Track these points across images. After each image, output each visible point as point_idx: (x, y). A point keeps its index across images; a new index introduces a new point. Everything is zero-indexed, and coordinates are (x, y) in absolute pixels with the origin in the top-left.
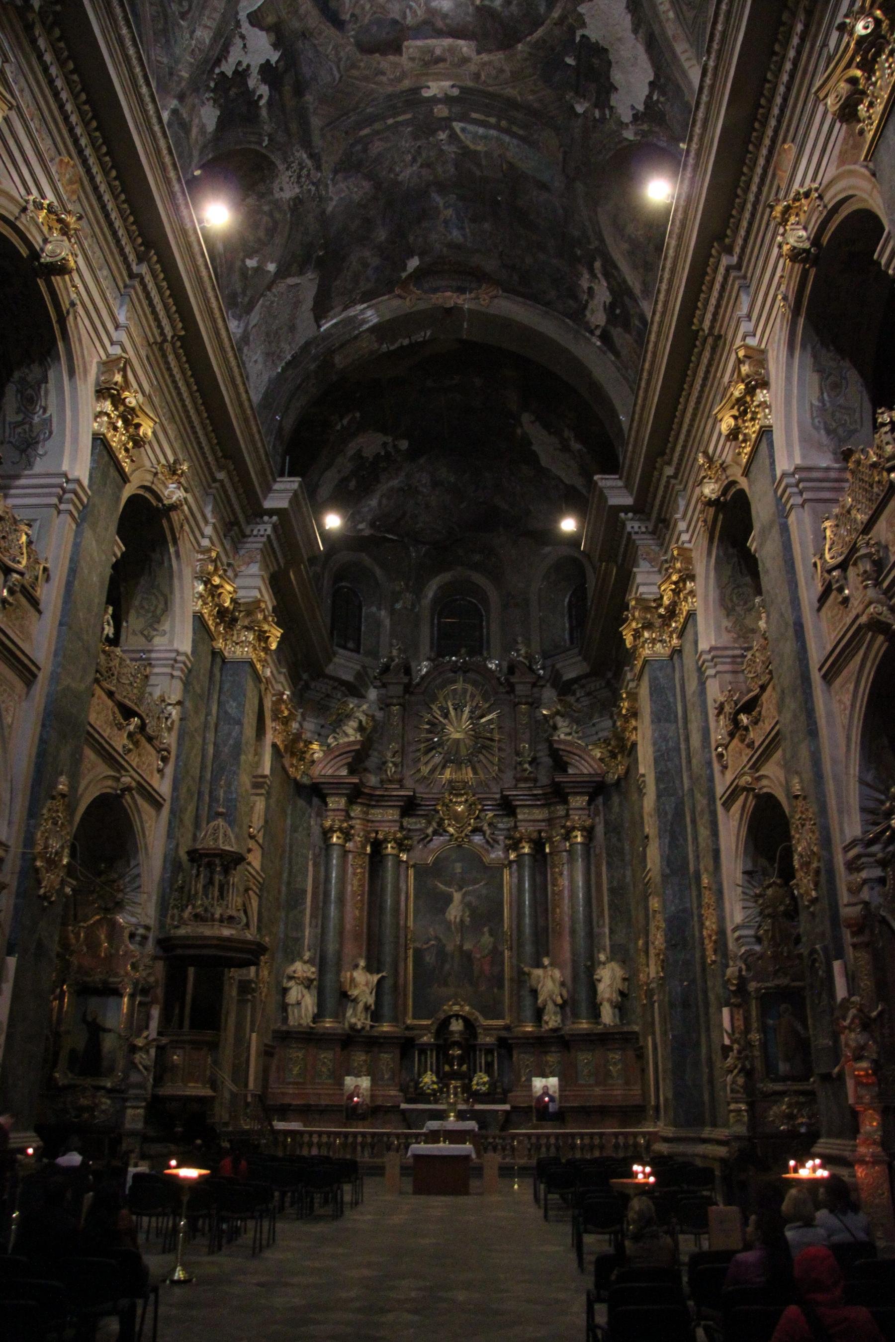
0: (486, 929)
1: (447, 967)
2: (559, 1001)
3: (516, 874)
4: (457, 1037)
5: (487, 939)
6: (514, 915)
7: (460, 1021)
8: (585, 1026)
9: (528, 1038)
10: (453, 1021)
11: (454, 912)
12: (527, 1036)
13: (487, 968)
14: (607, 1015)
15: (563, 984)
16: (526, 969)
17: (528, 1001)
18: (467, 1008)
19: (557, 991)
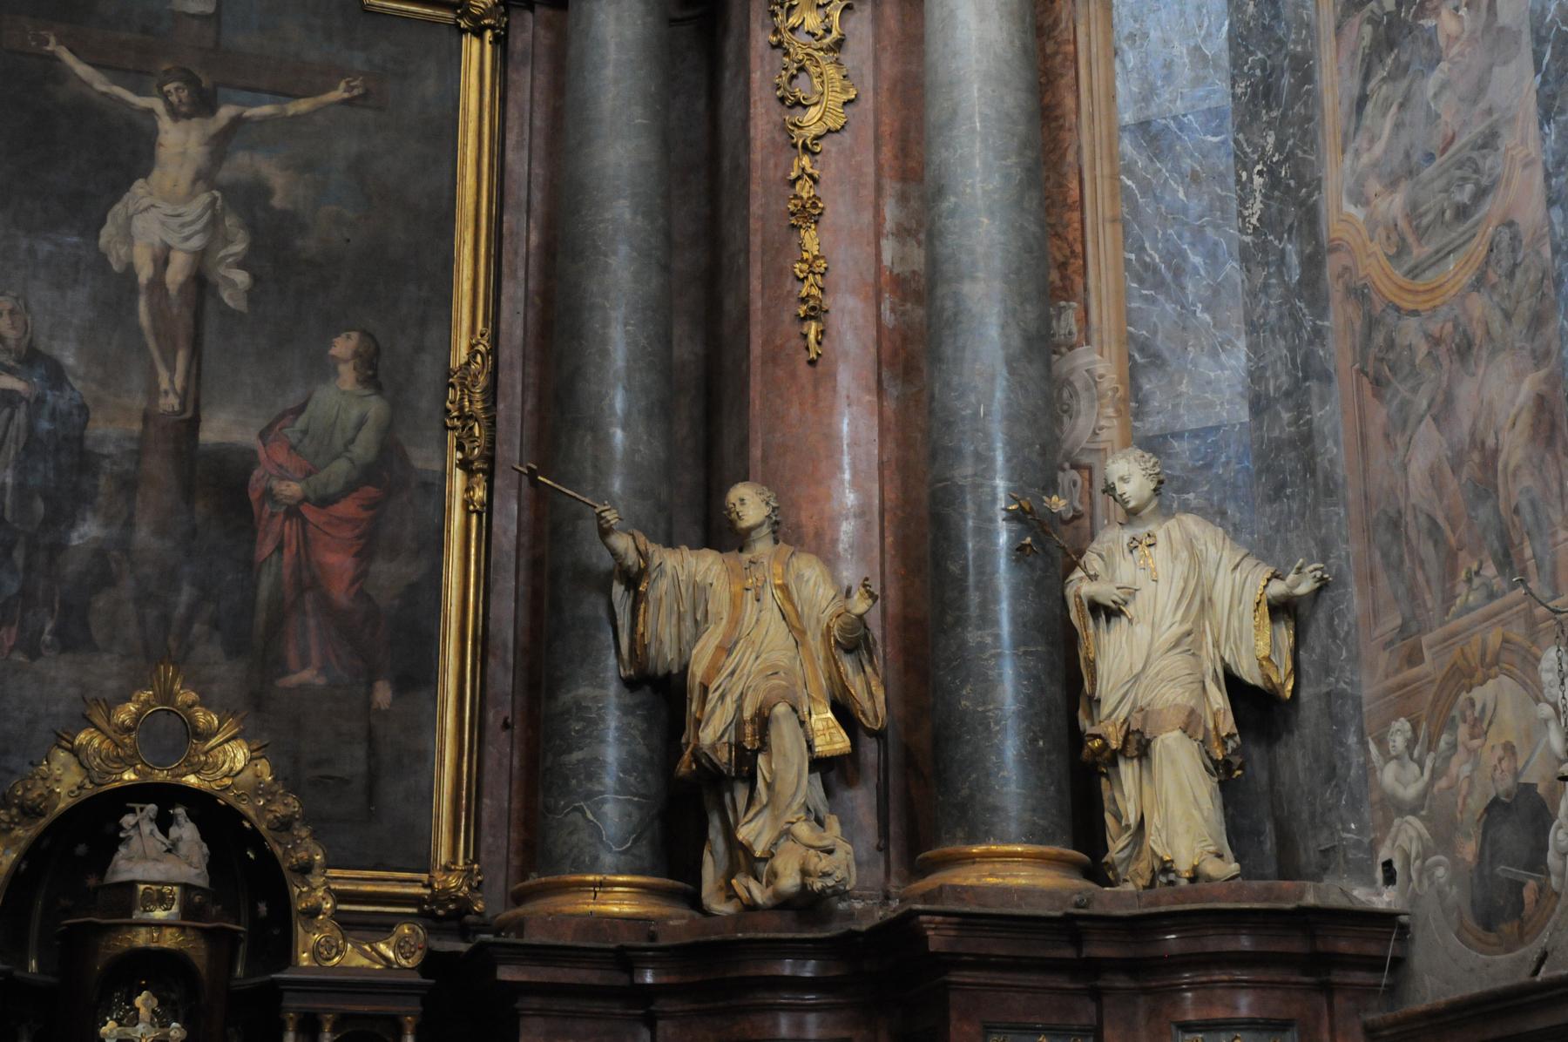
0: (344, 346)
1: (88, 531)
2: (831, 739)
3: (524, 81)
4: (159, 926)
5: (342, 400)
6: (514, 291)
7: (186, 831)
8: (1022, 877)
9: (626, 959)
10: (139, 823)
11: (160, 221)
12: (618, 951)
13: (337, 562)
14: (1174, 817)
15: (854, 641)
16: (622, 542)
17: (611, 743)
18: (238, 755)
19: (820, 682)
